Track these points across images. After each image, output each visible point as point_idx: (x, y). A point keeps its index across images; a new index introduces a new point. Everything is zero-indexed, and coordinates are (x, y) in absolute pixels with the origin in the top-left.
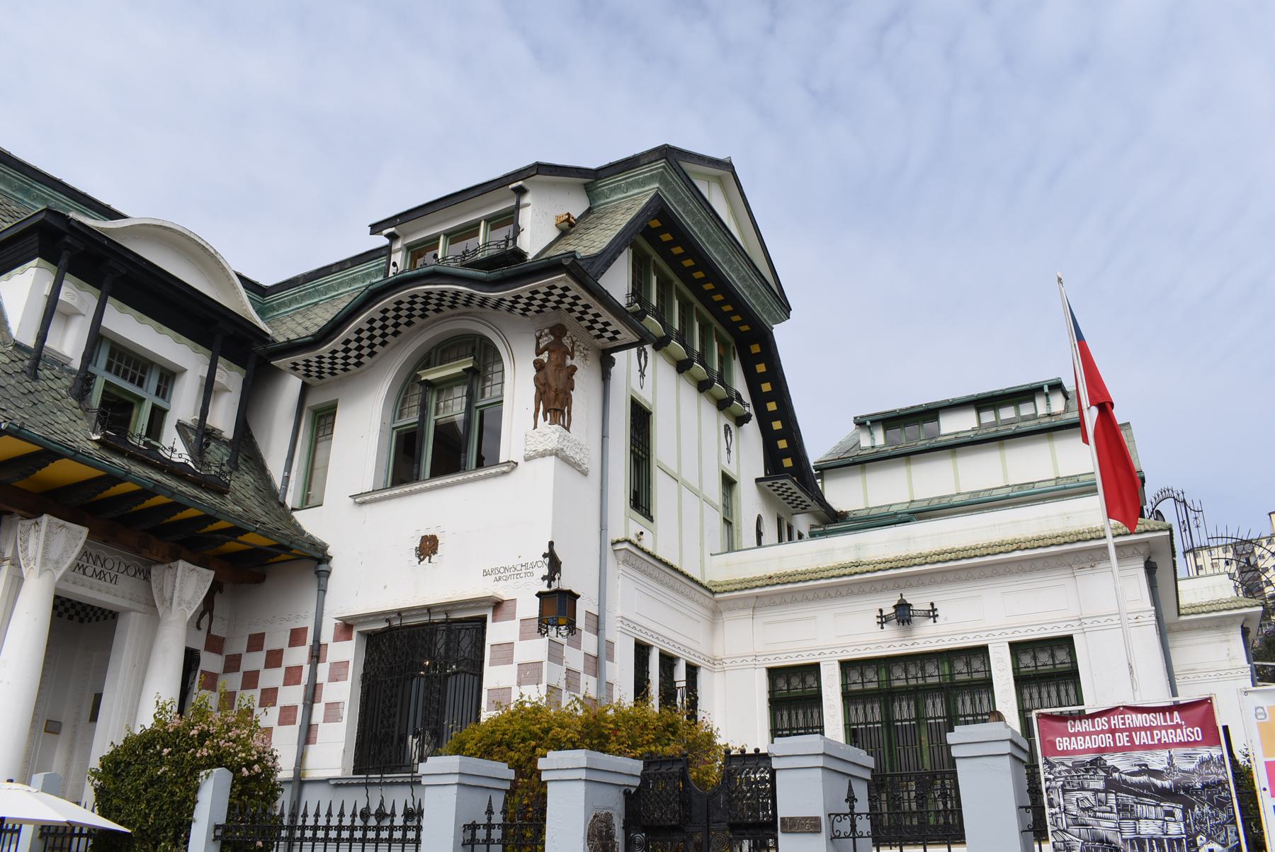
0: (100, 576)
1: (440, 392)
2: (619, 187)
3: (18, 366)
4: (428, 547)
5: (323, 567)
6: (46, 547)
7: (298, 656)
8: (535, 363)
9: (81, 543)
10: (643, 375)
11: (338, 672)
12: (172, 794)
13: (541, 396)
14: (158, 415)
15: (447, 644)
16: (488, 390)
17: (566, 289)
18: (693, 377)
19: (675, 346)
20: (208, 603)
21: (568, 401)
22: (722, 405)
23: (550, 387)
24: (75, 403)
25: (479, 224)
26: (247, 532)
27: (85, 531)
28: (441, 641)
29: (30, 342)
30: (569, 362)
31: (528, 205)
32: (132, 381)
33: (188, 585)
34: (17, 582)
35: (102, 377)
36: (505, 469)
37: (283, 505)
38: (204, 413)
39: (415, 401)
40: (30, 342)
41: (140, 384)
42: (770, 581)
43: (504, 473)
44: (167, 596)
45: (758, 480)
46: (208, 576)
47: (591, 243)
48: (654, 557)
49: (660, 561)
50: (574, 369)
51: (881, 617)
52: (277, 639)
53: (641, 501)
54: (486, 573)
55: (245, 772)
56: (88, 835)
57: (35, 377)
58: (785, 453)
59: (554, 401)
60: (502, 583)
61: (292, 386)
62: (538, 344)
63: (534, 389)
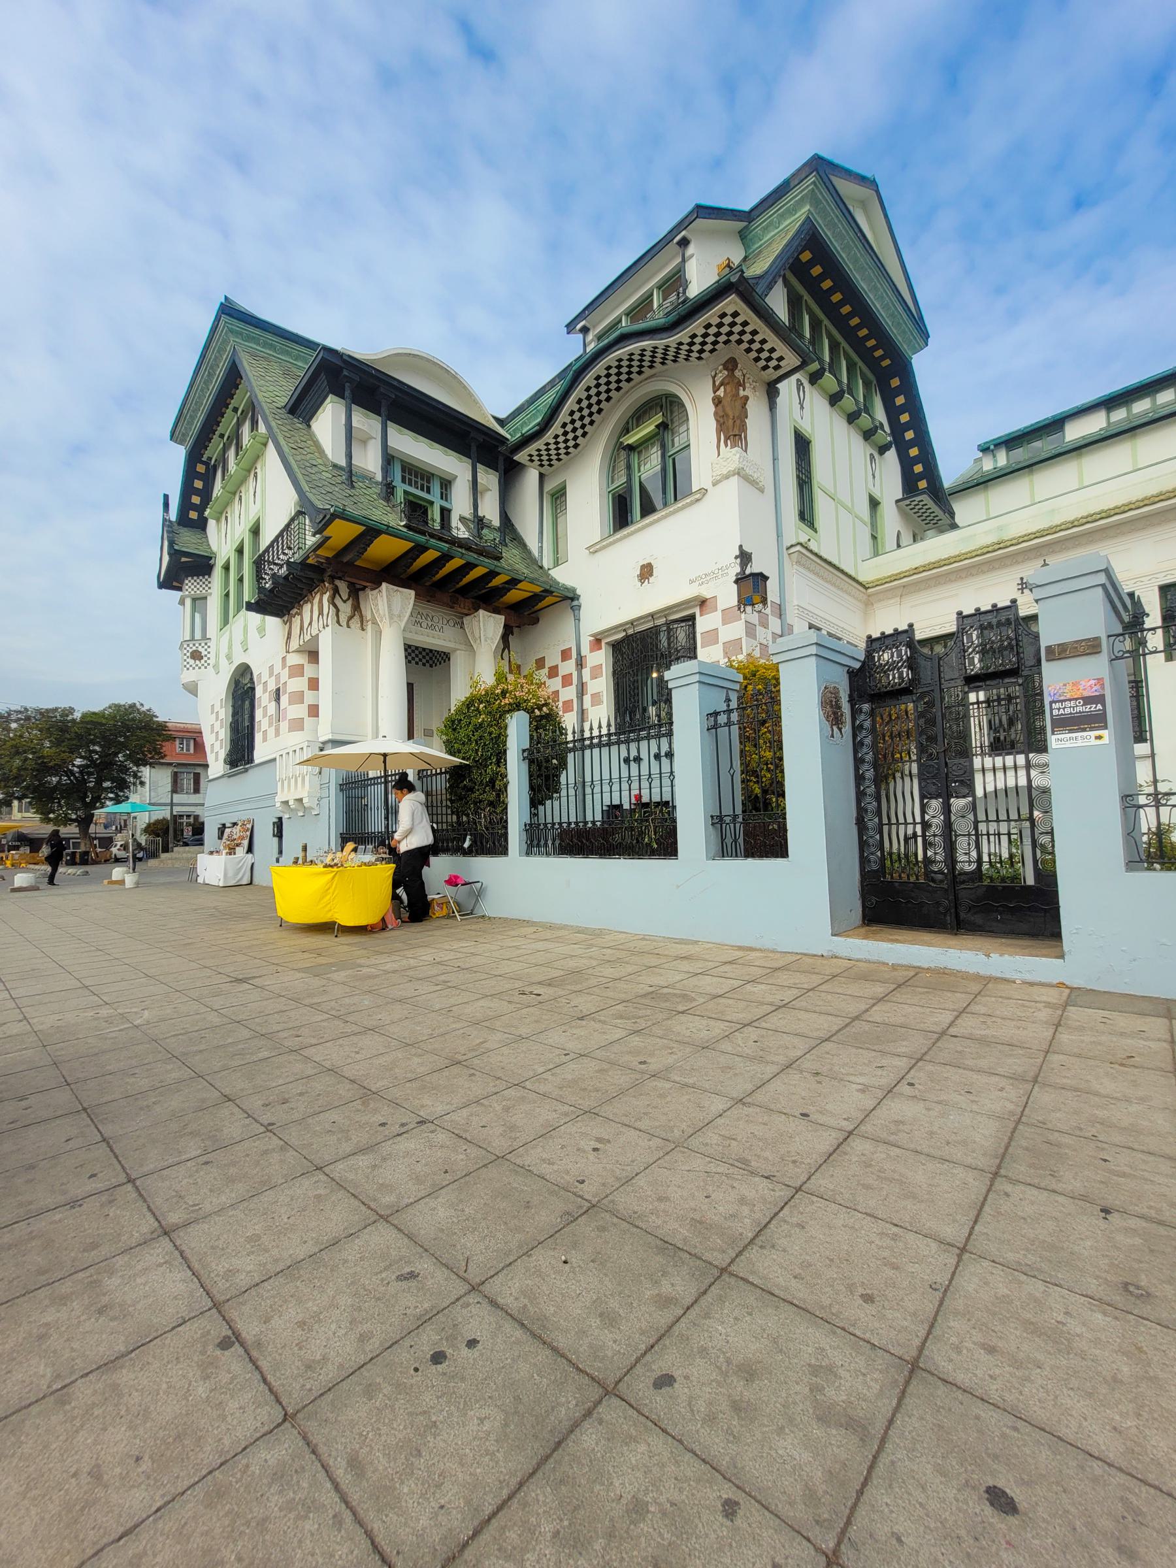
0: (432, 627)
1: (640, 453)
2: (771, 223)
3: (339, 480)
4: (646, 572)
5: (575, 603)
7: (569, 667)
8: (713, 400)
9: (412, 601)
10: (802, 408)
11: (596, 672)
12: (490, 733)
13: (721, 426)
14: (445, 513)
15: (669, 639)
16: (676, 439)
17: (735, 314)
18: (842, 410)
19: (828, 378)
20: (505, 638)
21: (743, 428)
22: (868, 435)
23: (727, 416)
25: (652, 295)
26: (520, 581)
27: (413, 593)
28: (663, 638)
29: (343, 462)
30: (742, 393)
31: (692, 256)
32: (422, 489)
33: (488, 626)
34: (378, 634)
35: (401, 488)
36: (697, 496)
37: (541, 567)
39: (622, 465)
40: (343, 462)
41: (428, 492)
42: (917, 571)
43: (698, 500)
44: (477, 636)
45: (897, 501)
46: (500, 619)
47: (756, 269)
48: (820, 557)
49: (825, 561)
50: (746, 398)
51: (1022, 584)
52: (553, 659)
53: (806, 515)
54: (692, 582)
55: (537, 712)
56: (446, 773)
57: (353, 487)
58: (920, 476)
59: (732, 428)
60: (705, 586)
61: (531, 477)
62: (714, 382)
63: (714, 423)
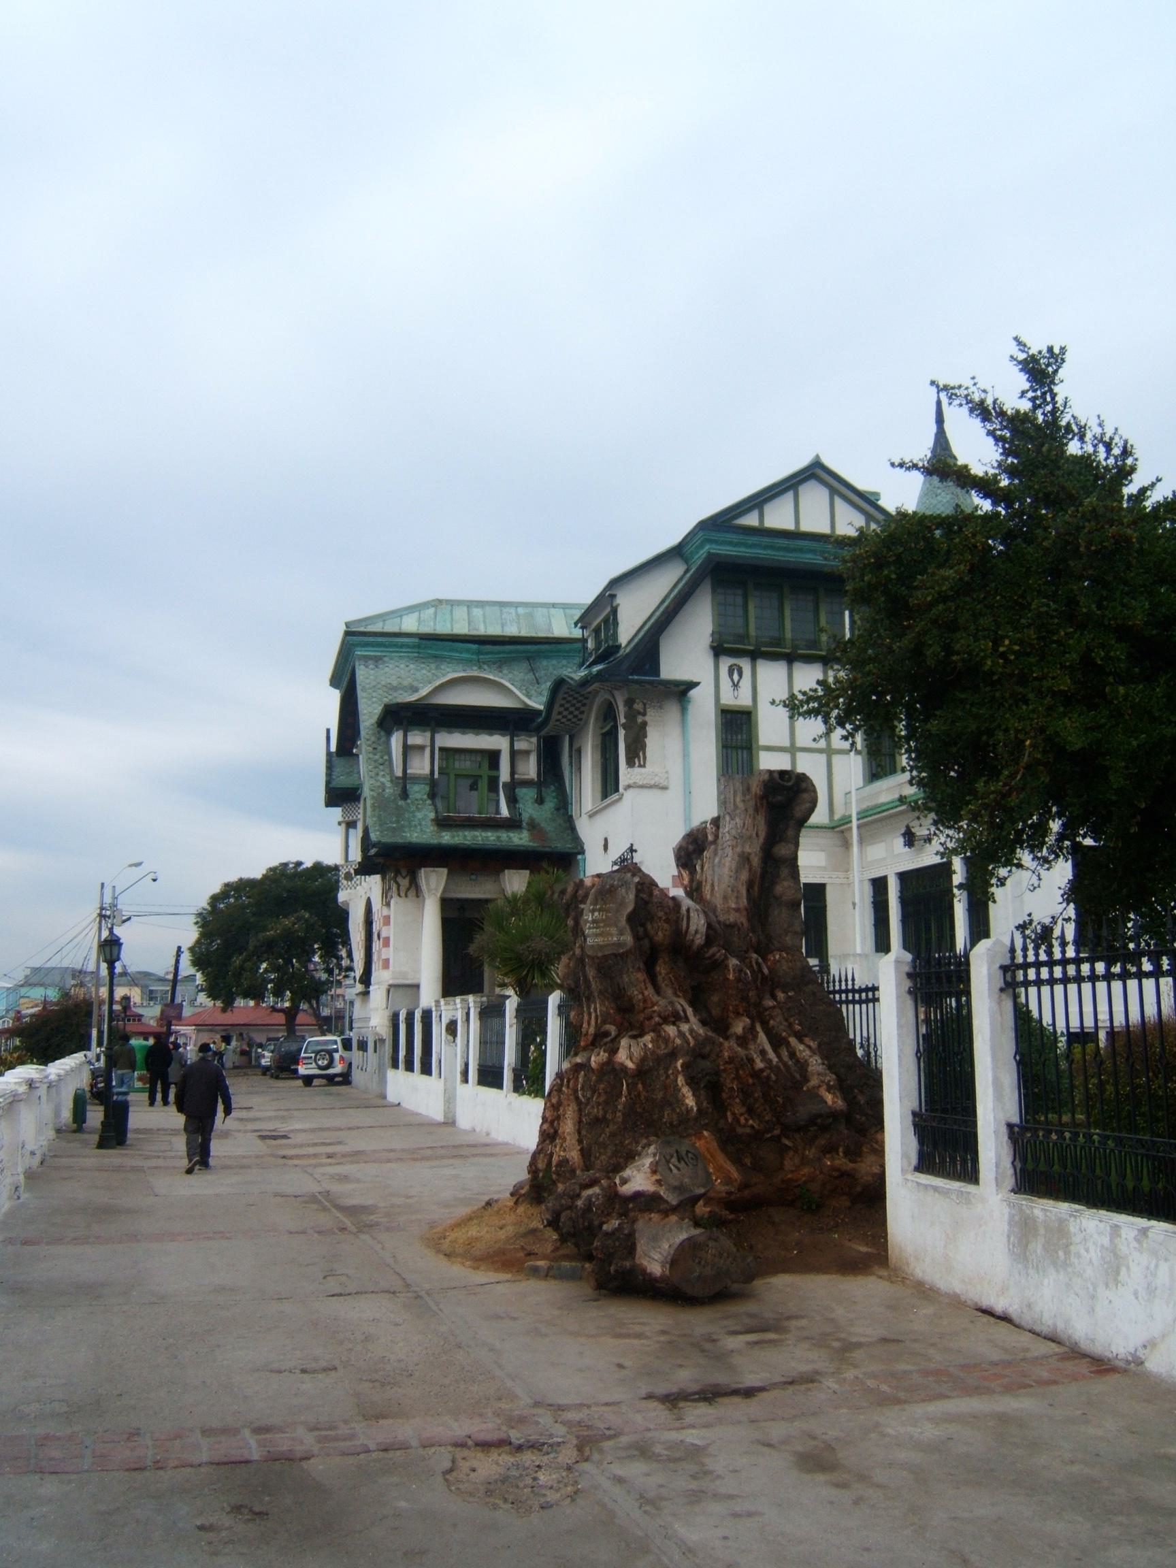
5: (579, 857)
6: (428, 884)
9: (445, 877)
10: (736, 686)
21: (643, 747)
24: (429, 802)
38: (513, 773)
43: (620, 799)
50: (645, 724)
